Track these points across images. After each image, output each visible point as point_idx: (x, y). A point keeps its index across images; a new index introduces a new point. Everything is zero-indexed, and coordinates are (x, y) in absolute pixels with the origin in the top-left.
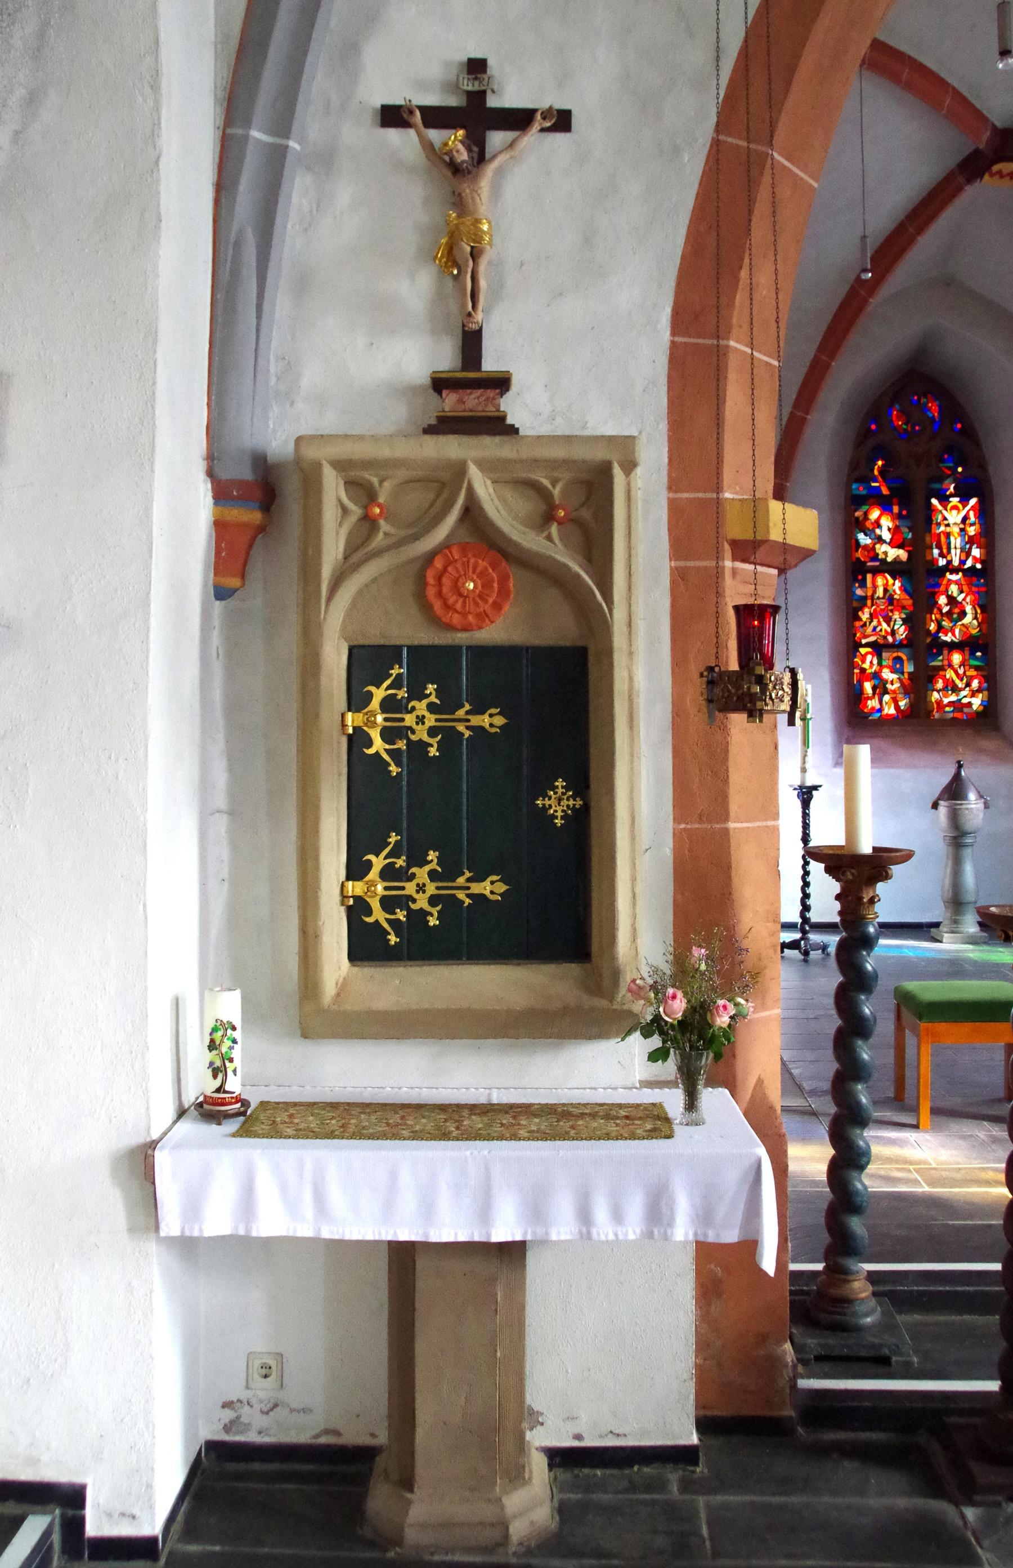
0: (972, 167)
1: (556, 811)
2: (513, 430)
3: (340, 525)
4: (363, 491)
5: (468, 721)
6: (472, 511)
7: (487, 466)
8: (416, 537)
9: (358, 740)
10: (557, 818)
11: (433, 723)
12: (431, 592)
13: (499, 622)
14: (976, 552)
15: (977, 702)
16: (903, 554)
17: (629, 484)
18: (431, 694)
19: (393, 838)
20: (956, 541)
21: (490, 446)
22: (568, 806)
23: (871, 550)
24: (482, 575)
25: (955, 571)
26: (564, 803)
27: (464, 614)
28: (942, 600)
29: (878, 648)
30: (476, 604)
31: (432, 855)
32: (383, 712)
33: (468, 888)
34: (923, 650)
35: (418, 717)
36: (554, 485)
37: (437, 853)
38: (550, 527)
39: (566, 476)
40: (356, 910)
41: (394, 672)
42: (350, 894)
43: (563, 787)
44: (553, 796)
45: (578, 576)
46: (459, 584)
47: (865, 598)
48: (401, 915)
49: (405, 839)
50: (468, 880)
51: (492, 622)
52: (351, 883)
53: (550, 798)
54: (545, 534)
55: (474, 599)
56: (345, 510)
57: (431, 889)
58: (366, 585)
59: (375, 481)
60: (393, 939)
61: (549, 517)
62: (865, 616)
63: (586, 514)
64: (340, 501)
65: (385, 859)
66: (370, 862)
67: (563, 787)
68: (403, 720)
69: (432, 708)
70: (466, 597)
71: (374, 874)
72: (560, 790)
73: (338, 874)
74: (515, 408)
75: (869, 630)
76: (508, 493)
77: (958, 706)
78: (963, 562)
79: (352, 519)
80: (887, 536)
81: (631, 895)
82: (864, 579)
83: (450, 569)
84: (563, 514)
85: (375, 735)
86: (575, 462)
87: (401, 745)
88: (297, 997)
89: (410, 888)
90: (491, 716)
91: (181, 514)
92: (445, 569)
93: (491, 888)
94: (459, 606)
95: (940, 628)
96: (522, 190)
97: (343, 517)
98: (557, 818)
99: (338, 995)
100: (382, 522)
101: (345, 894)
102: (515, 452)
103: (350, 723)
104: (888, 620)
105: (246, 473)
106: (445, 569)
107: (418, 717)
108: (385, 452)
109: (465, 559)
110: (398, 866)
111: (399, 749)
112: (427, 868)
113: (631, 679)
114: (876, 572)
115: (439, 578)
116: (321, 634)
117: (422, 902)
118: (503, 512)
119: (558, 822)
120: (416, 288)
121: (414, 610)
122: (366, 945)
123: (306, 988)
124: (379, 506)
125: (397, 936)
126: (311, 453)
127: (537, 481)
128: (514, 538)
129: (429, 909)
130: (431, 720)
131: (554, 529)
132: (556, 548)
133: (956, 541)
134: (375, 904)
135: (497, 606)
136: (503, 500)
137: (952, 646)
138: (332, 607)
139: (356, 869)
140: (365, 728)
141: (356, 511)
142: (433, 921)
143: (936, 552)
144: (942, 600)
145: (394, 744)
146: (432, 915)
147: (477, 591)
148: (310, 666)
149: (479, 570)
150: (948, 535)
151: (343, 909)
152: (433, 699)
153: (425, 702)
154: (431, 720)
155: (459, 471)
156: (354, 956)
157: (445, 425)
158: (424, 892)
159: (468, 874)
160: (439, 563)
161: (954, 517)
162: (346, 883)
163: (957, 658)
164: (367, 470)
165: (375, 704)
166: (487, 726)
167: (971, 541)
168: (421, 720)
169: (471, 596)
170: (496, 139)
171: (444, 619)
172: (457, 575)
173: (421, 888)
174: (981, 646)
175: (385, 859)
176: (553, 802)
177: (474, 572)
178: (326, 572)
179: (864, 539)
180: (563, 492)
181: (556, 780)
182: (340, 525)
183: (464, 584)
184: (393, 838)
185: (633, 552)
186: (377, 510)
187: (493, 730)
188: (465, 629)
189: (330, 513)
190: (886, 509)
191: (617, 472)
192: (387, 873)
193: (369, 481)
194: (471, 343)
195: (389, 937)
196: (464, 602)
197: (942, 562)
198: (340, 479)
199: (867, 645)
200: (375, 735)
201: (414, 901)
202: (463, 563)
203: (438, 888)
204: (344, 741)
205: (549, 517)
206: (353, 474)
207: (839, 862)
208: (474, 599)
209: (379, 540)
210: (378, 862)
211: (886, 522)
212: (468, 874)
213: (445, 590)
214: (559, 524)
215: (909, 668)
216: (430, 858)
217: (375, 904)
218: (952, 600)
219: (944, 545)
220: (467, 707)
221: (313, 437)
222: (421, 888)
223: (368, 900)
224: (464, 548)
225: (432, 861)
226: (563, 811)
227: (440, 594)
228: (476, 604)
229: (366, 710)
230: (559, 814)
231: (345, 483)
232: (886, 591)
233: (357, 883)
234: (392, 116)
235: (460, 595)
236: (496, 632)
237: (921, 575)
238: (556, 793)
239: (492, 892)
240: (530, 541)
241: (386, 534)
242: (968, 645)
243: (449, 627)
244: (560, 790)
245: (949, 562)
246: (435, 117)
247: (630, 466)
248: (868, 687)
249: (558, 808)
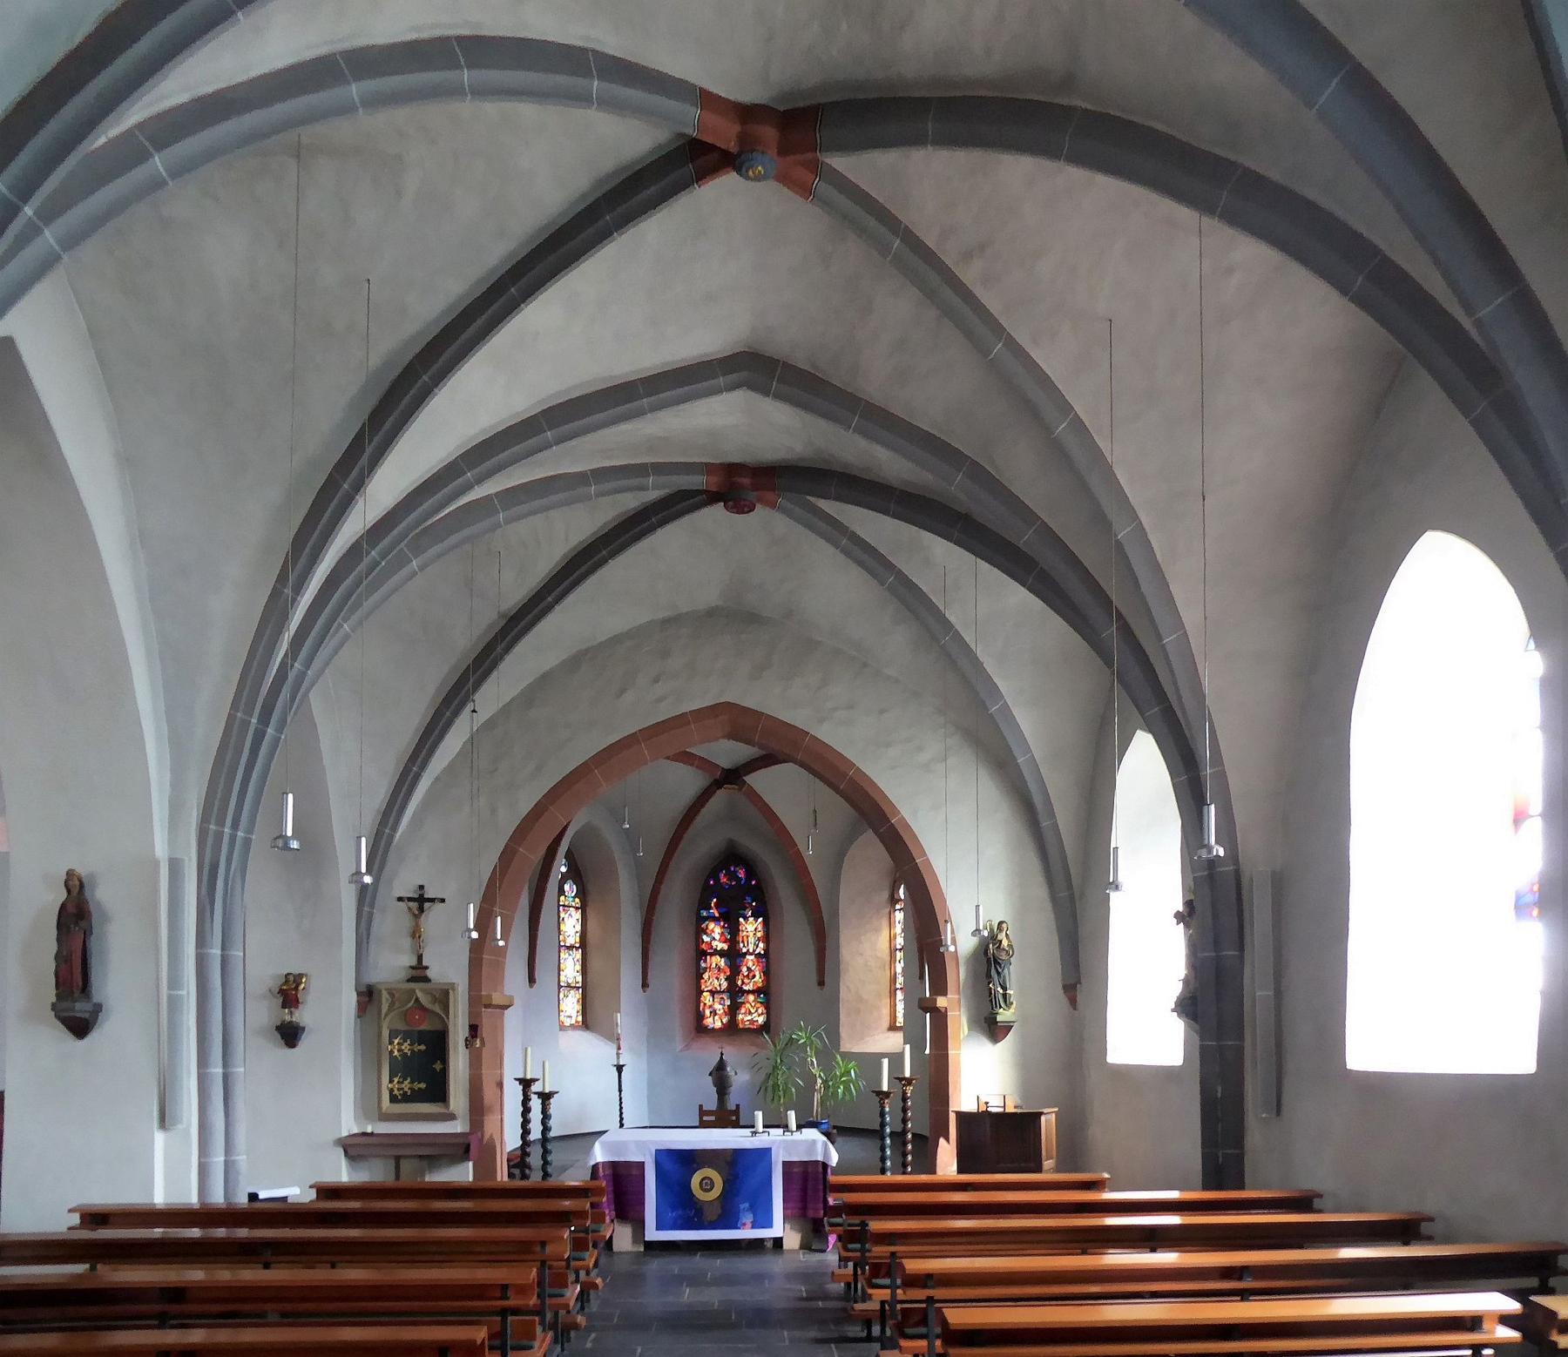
0: (717, 784)
4: (391, 994)
15: (761, 1020)
16: (725, 946)
20: (752, 940)
21: (421, 985)
29: (713, 993)
34: (735, 992)
40: (391, 1091)
62: (706, 976)
74: (429, 973)
77: (752, 1022)
80: (717, 937)
91: (350, 999)
93: (423, 1086)
96: (434, 918)
105: (364, 989)
120: (407, 942)
122: (393, 1099)
132: (437, 1008)
133: (752, 940)
137: (749, 992)
139: (391, 1081)
144: (744, 969)
148: (380, 1035)
155: (413, 991)
157: (412, 979)
161: (751, 928)
163: (751, 998)
168: (406, 1047)
170: (427, 905)
173: (406, 1085)
174: (763, 992)
178: (384, 1010)
194: (420, 958)
207: (521, 1081)
211: (718, 930)
215: (728, 1003)
219: (745, 940)
234: (400, 899)
236: (422, 1027)
237: (734, 955)
242: (755, 992)
246: (410, 899)
248: (707, 1012)
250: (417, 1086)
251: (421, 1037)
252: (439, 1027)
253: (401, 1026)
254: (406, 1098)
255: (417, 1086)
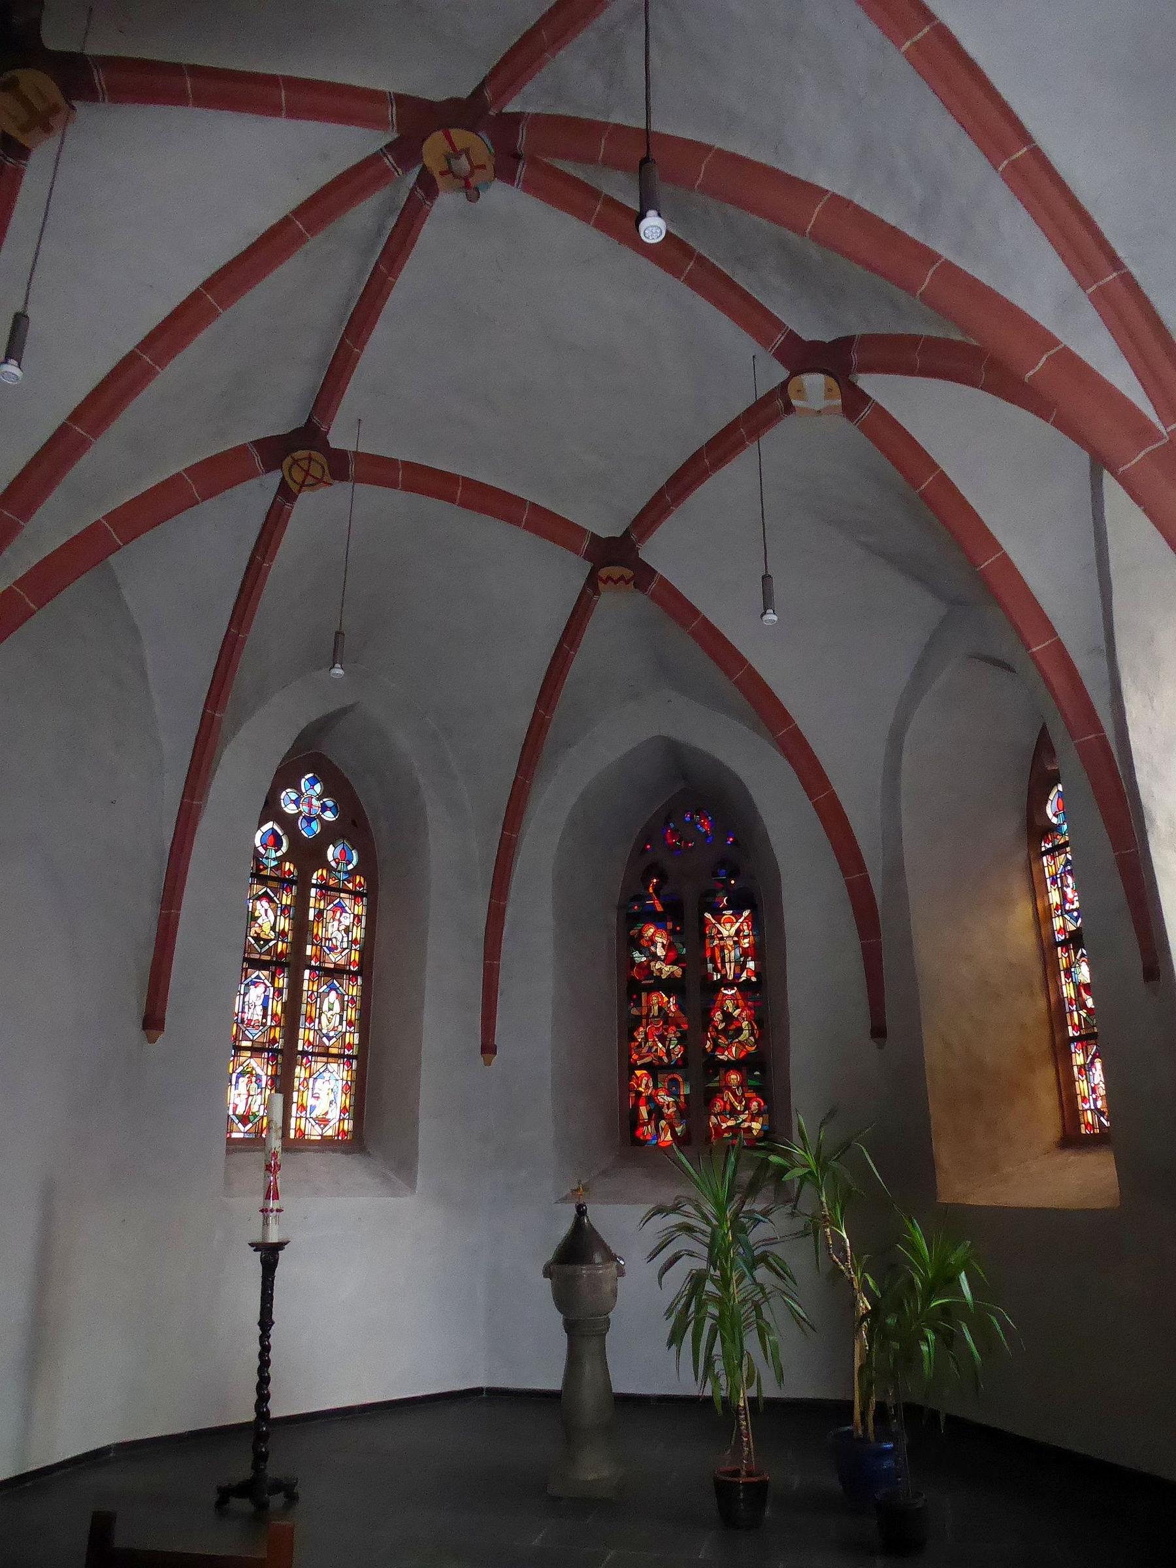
14: (751, 965)
23: (646, 969)
25: (730, 985)
28: (718, 1016)
29: (654, 1069)
47: (640, 1017)
75: (645, 1050)
78: (737, 976)
80: (660, 952)
82: (640, 997)
95: (716, 1046)
104: (663, 1039)
114: (650, 990)
133: (732, 954)
137: (730, 1066)
143: (710, 966)
144: (718, 1016)
150: (722, 949)
161: (730, 929)
163: (734, 1077)
167: (745, 953)
179: (639, 958)
190: (660, 926)
197: (716, 977)
199: (641, 1067)
211: (660, 940)
218: (727, 1016)
232: (660, 1009)
245: (724, 976)
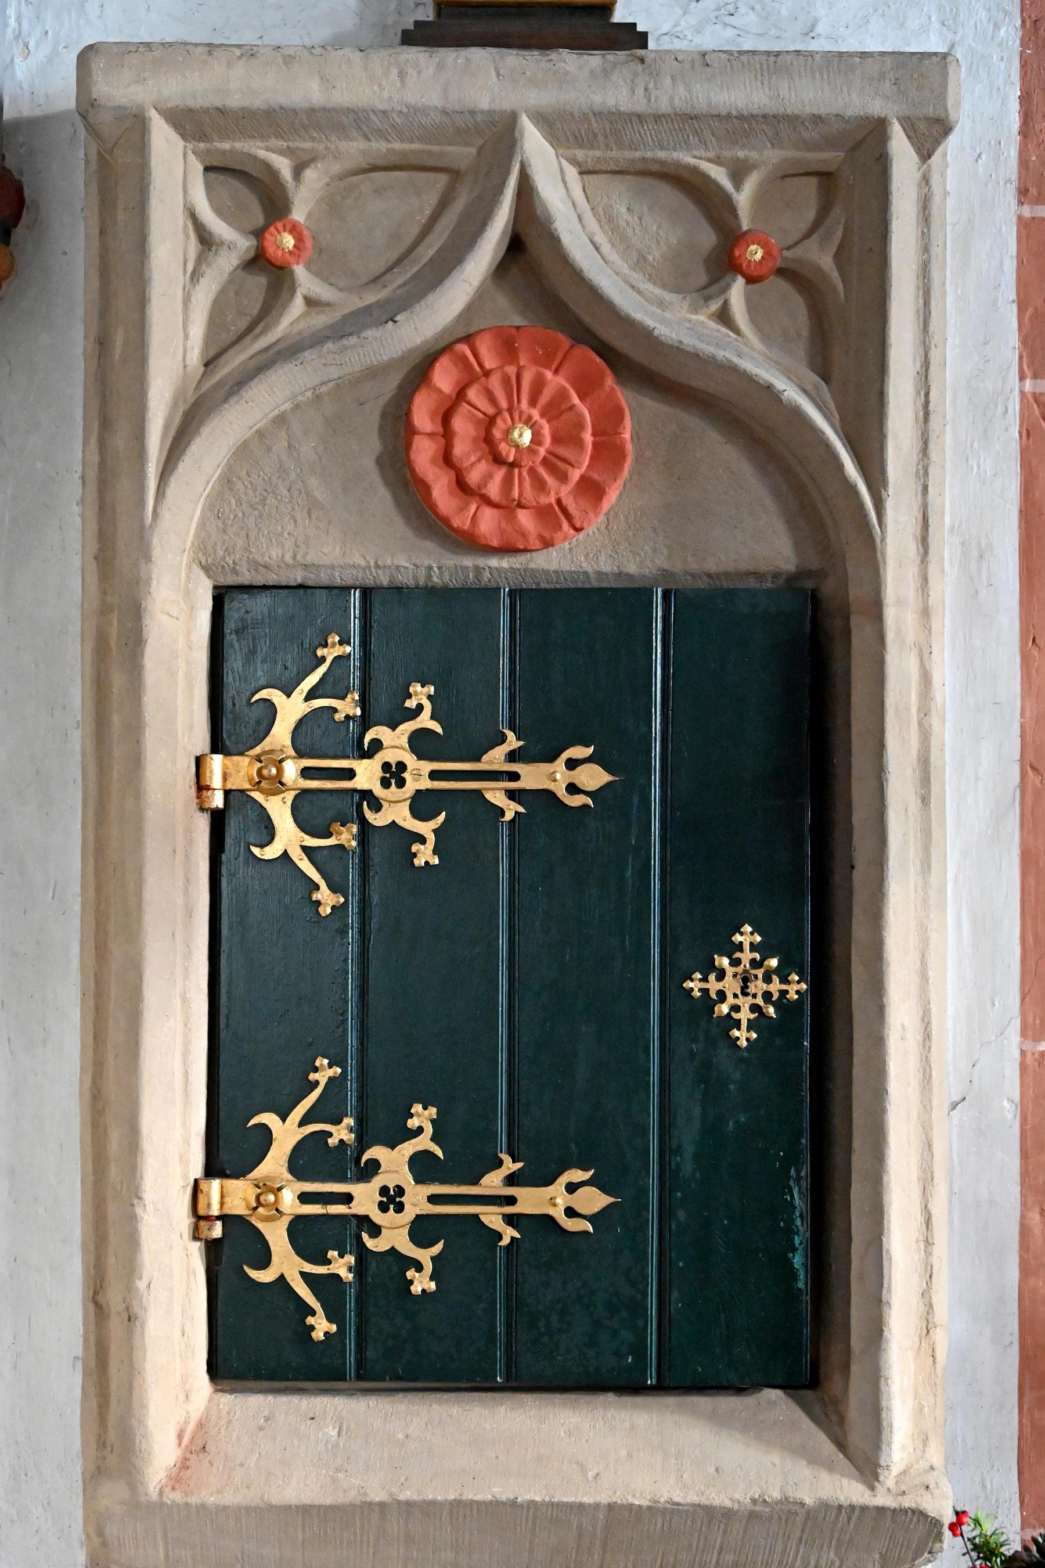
1: (736, 1008)
2: (632, 38)
3: (195, 276)
5: (514, 776)
6: (528, 251)
7: (563, 128)
8: (388, 313)
9: (231, 825)
10: (737, 1024)
11: (426, 784)
12: (424, 454)
13: (595, 525)
17: (926, 180)
18: (420, 708)
19: (324, 1073)
21: (577, 78)
22: (767, 996)
24: (556, 409)
26: (758, 987)
27: (507, 507)
30: (540, 486)
31: (422, 1117)
32: (300, 754)
33: (511, 1200)
35: (386, 766)
36: (738, 177)
37: (433, 1111)
38: (727, 287)
39: (770, 156)
40: (229, 1251)
41: (330, 653)
42: (215, 1211)
43: (753, 947)
44: (730, 971)
45: (796, 412)
46: (497, 433)
48: (342, 1266)
49: (352, 1074)
50: (511, 1180)
51: (578, 530)
52: (216, 1184)
53: (721, 975)
54: (715, 306)
55: (532, 471)
56: (206, 239)
57: (417, 1200)
58: (260, 434)
59: (283, 166)
60: (321, 1326)
61: (724, 263)
63: (822, 258)
64: (193, 216)
65: (302, 1123)
66: (265, 1129)
67: (753, 947)
68: (350, 774)
69: (422, 744)
70: (512, 465)
71: (274, 1164)
72: (746, 956)
73: (183, 1160)
76: (619, 198)
79: (226, 262)
81: (920, 1219)
83: (472, 394)
84: (759, 256)
85: (279, 810)
86: (793, 120)
87: (346, 836)
88: (77, 1470)
89: (365, 1198)
90: (572, 764)
92: (460, 395)
93: (572, 1200)
94: (494, 490)
97: (200, 259)
98: (737, 1024)
99: (184, 1464)
100: (300, 271)
101: (202, 1212)
102: (640, 91)
103: (216, 782)
106: (460, 395)
107: (386, 766)
108: (307, 91)
109: (512, 370)
110: (332, 1142)
111: (341, 847)
112: (409, 1148)
113: (926, 678)
115: (446, 418)
116: (146, 555)
117: (394, 1235)
118: (606, 248)
119: (742, 1036)
121: (381, 497)
122: (254, 1342)
123: (102, 1443)
124: (294, 229)
125: (330, 1319)
126: (117, 89)
127: (695, 170)
128: (638, 316)
129: (409, 1249)
130: (419, 774)
131: (737, 291)
132: (749, 345)
134: (277, 1236)
135: (591, 490)
136: (608, 220)
138: (173, 489)
139: (228, 1149)
140: (256, 795)
141: (235, 242)
142: (421, 1283)
145: (329, 835)
146: (419, 1268)
147: (542, 451)
149: (544, 398)
151: (196, 1251)
152: (425, 721)
153: (407, 728)
154: (419, 774)
155: (500, 137)
156: (225, 1366)
158: (400, 1208)
159: (510, 1166)
160: (444, 378)
162: (203, 1185)
164: (263, 137)
165: (281, 733)
166: (561, 792)
168: (394, 774)
169: (526, 463)
171: (456, 523)
172: (490, 410)
173: (394, 1196)
175: (302, 1123)
176: (731, 985)
177: (533, 402)
180: (761, 199)
181: (738, 930)
182: (195, 276)
183: (508, 432)
184: (324, 1073)
185: (934, 355)
186: (289, 241)
187: (576, 801)
188: (507, 550)
189: (168, 248)
191: (900, 148)
192: (308, 1159)
193: (268, 167)
195: (310, 1320)
196: (508, 481)
198: (192, 157)
200: (279, 810)
201: (376, 1231)
202: (506, 381)
203: (433, 1199)
204: (202, 825)
205: (724, 263)
206: (226, 146)
208: (532, 471)
209: (292, 317)
210: (286, 1133)
212: (510, 1166)
213: (460, 449)
214: (750, 280)
216: (413, 1123)
217: (277, 1236)
220: (513, 742)
221: (126, 49)
222: (394, 1196)
223: (260, 1225)
224: (508, 345)
225: (420, 1130)
226: (755, 1008)
227: (447, 458)
228: (540, 486)
229: (258, 750)
230: (745, 1015)
231: (207, 169)
233: (232, 1184)
235: (498, 460)
236: (584, 554)
238: (735, 963)
239: (570, 1212)
240: (676, 322)
241: (311, 302)
243: (469, 542)
244: (746, 956)
247: (931, 133)
249: (745, 1003)
250: (507, 1199)
251: (567, 656)
252: (753, 541)
253: (358, 544)
254: (391, 1337)
255: (507, 1199)
